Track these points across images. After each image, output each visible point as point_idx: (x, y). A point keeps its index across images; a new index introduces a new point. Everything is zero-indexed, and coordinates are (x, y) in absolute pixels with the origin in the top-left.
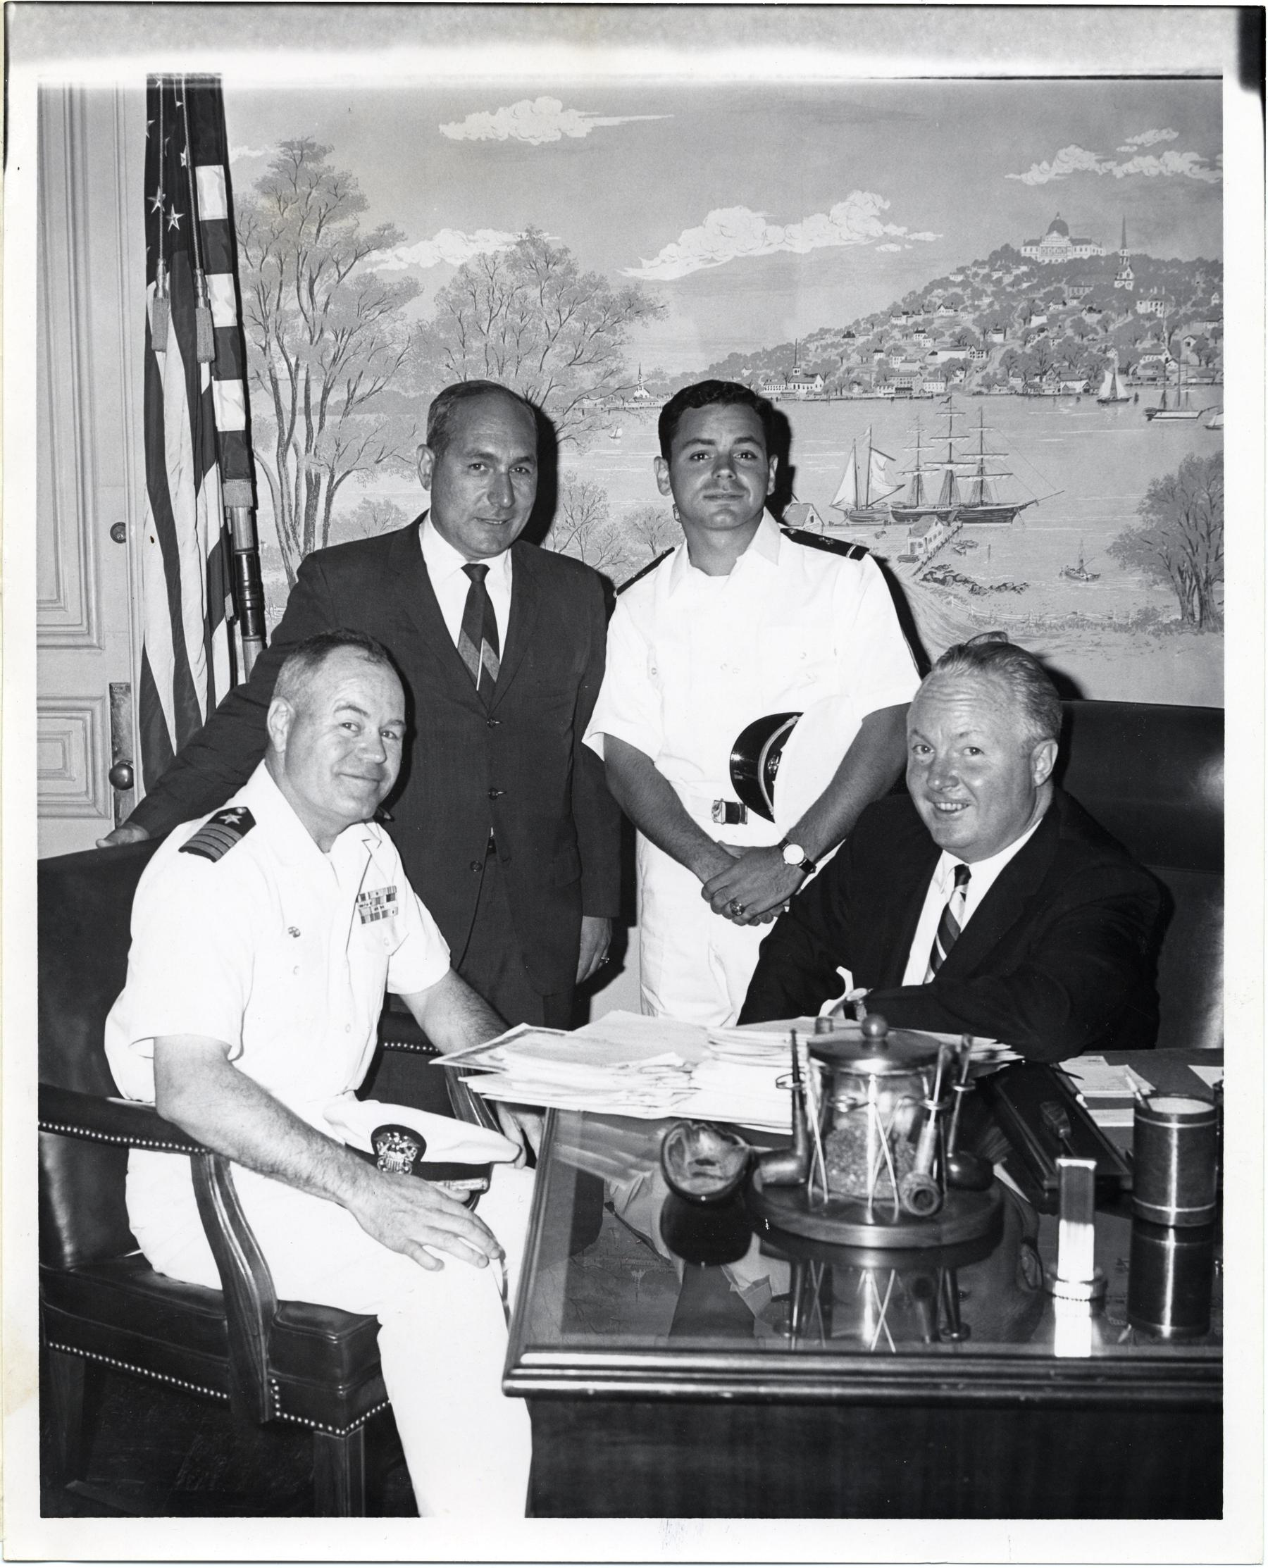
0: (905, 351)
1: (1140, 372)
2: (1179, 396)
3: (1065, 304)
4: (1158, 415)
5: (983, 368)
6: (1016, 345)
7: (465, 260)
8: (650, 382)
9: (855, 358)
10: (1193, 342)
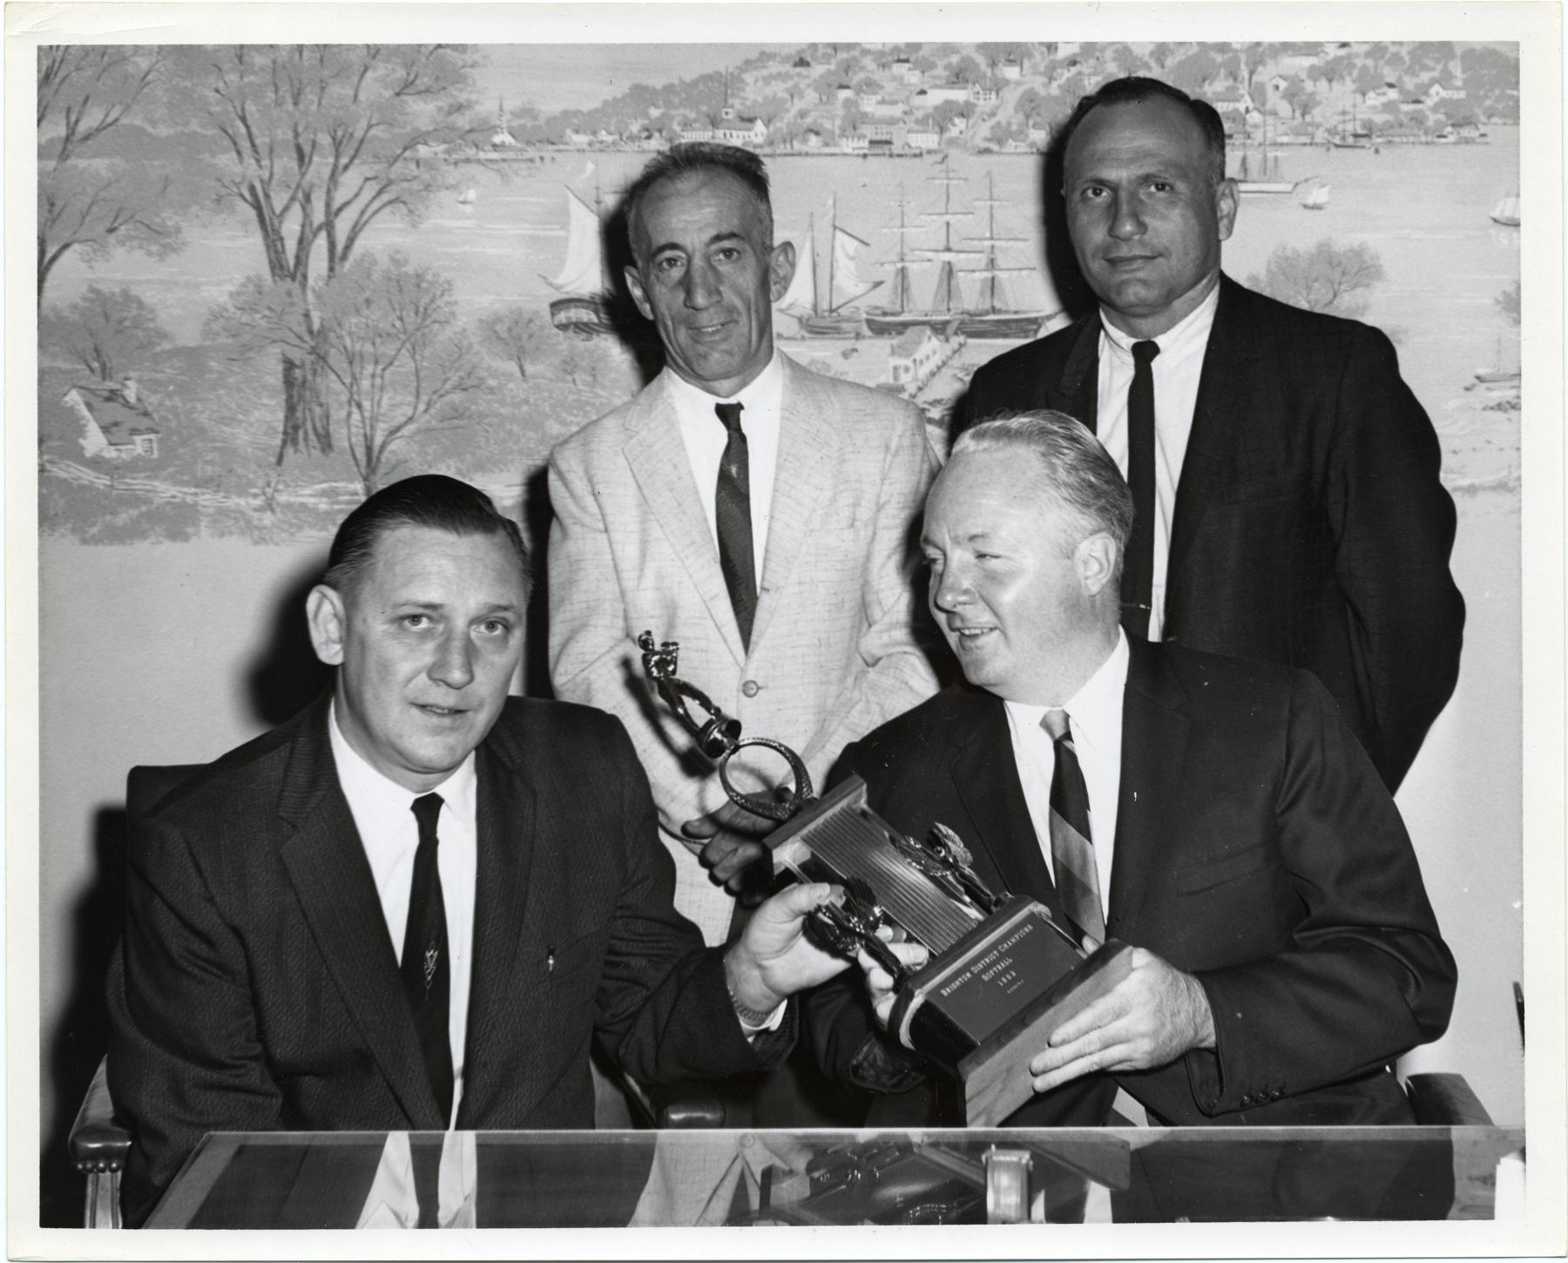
0: (881, 87)
2: (1265, 159)
5: (993, 114)
6: (1037, 83)
8: (516, 123)
9: (811, 96)
10: (1283, 85)
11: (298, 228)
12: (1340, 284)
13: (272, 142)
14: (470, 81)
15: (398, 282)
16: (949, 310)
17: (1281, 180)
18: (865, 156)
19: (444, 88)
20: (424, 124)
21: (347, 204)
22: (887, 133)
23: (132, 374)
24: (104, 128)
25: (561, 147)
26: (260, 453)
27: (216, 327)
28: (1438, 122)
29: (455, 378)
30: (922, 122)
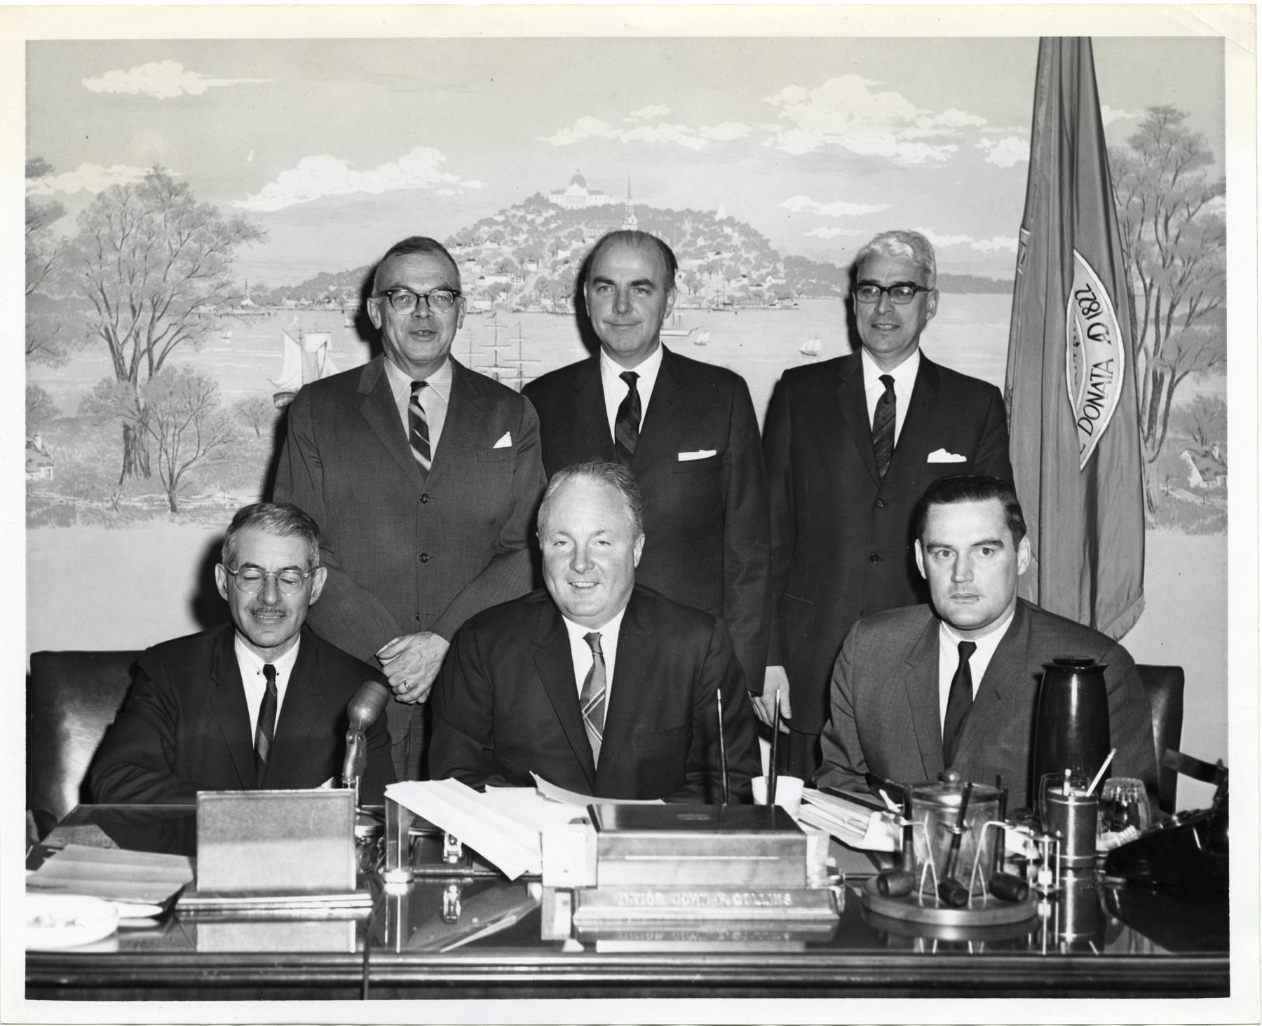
3: (584, 241)
5: (521, 290)
6: (546, 273)
7: (103, 189)
8: (254, 294)
11: (132, 351)
13: (118, 304)
14: (229, 270)
15: (188, 382)
20: (203, 295)
21: (159, 338)
23: (39, 433)
25: (280, 307)
26: (111, 478)
27: (86, 407)
28: (770, 297)
29: (220, 436)
30: (482, 294)
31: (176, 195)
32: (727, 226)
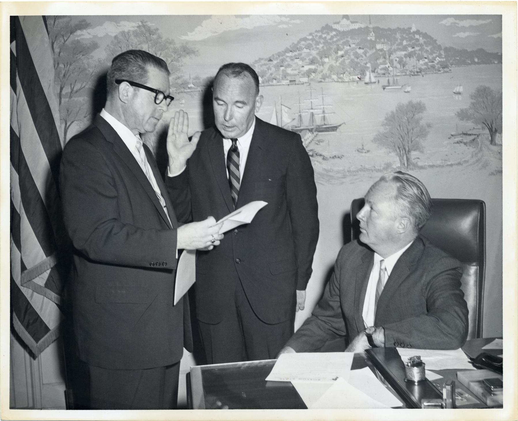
0: (292, 66)
1: (380, 72)
2: (394, 80)
3: (350, 46)
4: (387, 88)
5: (322, 71)
6: (333, 63)
8: (194, 81)
9: (273, 69)
10: (398, 59)
12: (415, 112)
16: (313, 125)
17: (399, 86)
18: (288, 85)
19: (174, 73)
22: (294, 78)
24: (81, 89)
28: (438, 67)
30: (304, 75)
31: (153, 35)
32: (417, 35)
